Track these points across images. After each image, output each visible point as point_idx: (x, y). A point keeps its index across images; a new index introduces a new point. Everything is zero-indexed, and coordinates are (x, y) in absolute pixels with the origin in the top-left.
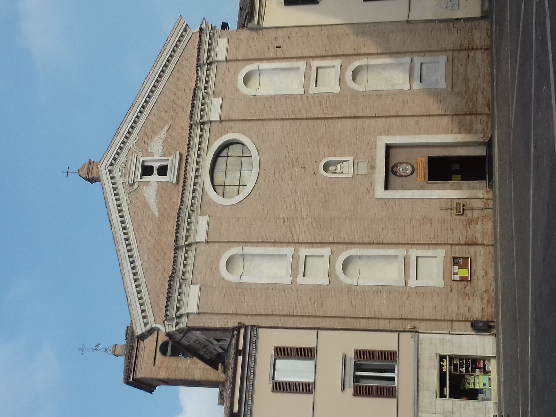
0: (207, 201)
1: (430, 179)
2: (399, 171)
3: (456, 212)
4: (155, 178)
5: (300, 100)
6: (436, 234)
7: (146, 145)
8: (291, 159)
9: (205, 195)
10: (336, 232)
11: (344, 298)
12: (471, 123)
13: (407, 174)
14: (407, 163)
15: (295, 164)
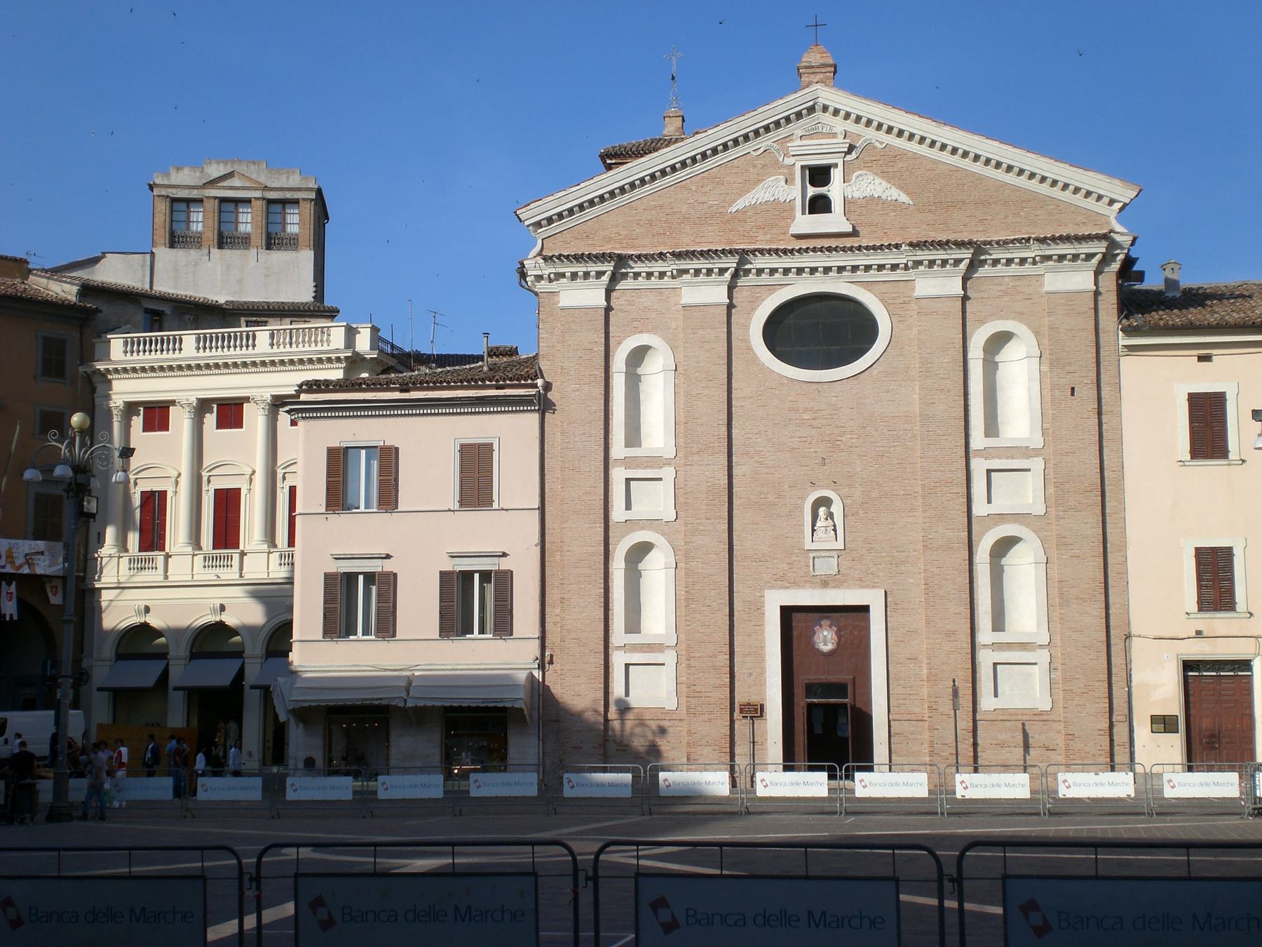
0: (758, 295)
6: (700, 695)
7: (868, 166)
9: (769, 290)
10: (702, 528)
11: (590, 548)
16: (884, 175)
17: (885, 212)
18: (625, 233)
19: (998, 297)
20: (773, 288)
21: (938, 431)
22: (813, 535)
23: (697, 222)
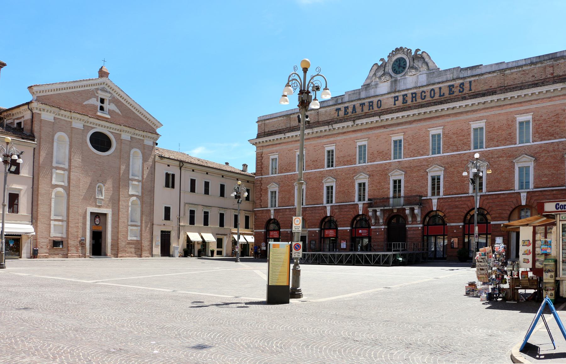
1: (93, 232)
4: (99, 104)
12: (114, 250)
16: (116, 105)
20: (93, 128)
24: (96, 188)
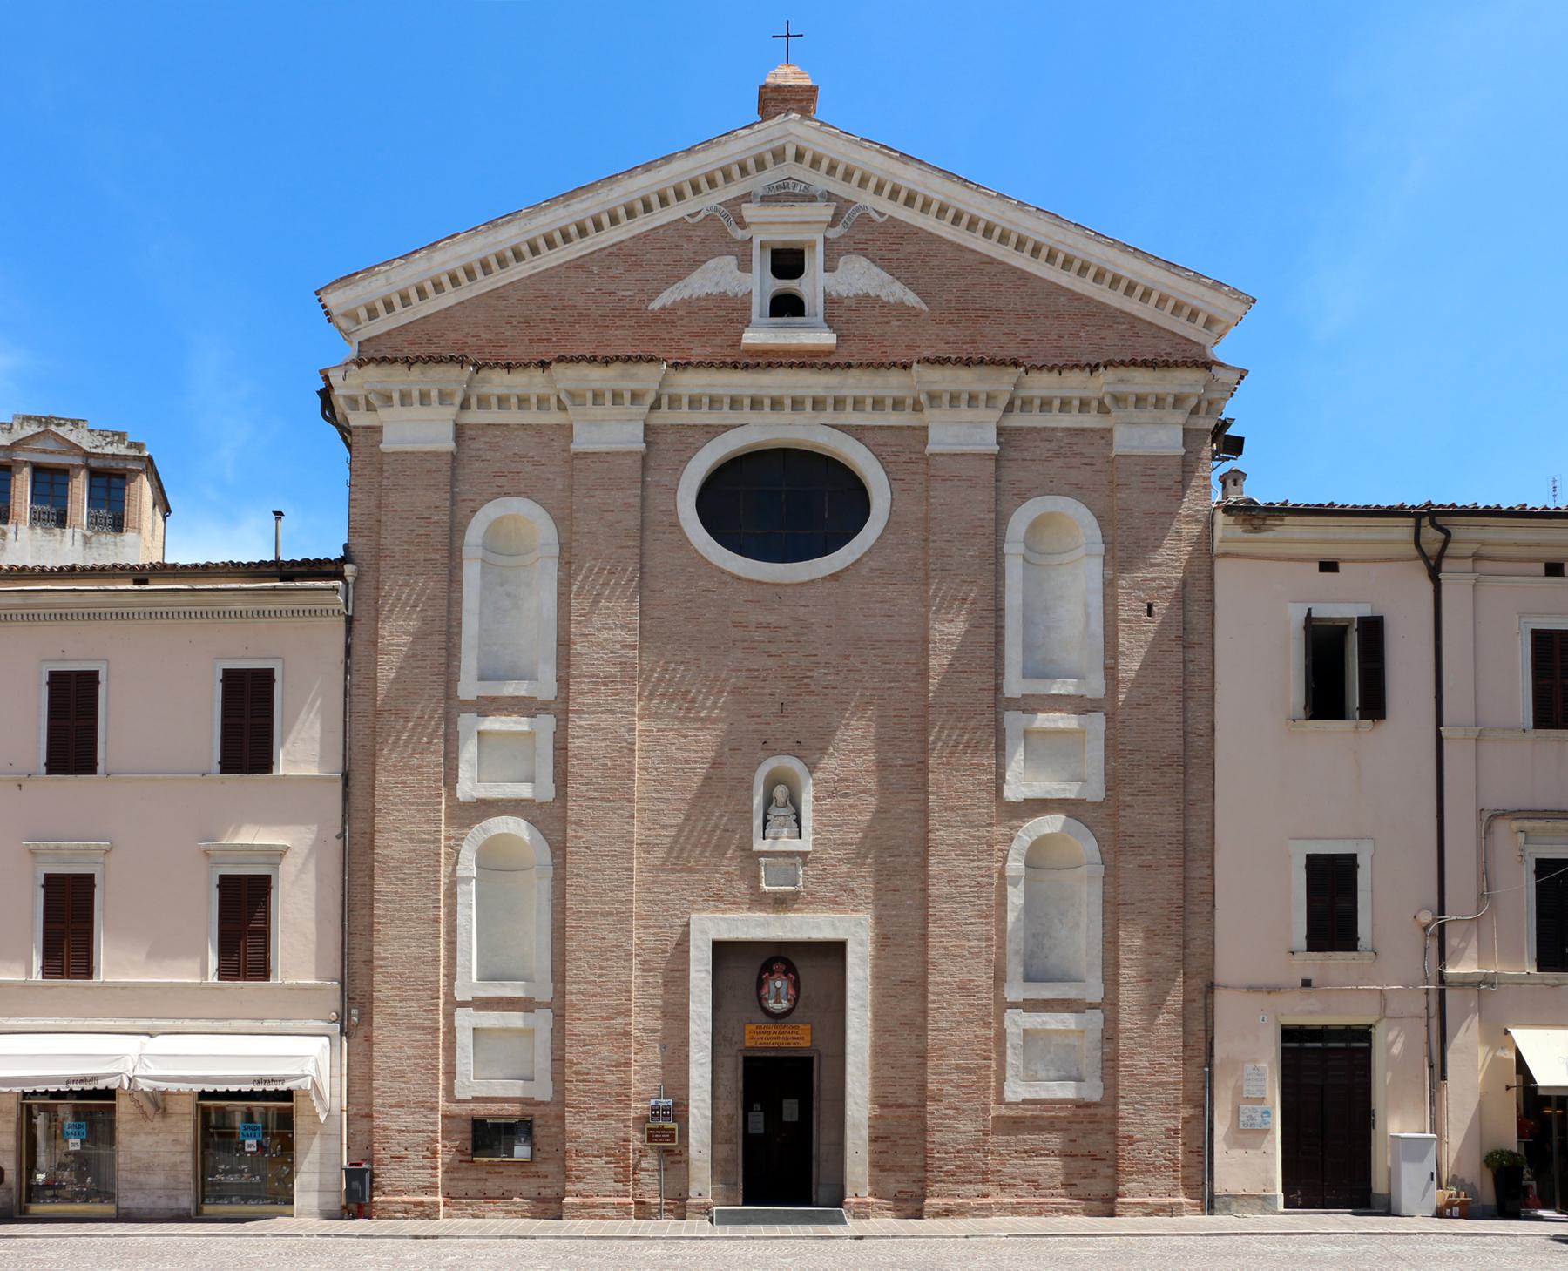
0: (691, 440)
2: (774, 977)
3: (649, 1129)
4: (761, 284)
5: (984, 686)
7: (859, 248)
8: (808, 674)
13: (764, 1001)
14: (796, 1001)
15: (794, 684)
16: (883, 262)
17: (886, 320)
18: (488, 337)
19: (1047, 460)
20: (712, 431)
21: (957, 665)
22: (764, 829)
23: (600, 322)
24: (750, 788)
